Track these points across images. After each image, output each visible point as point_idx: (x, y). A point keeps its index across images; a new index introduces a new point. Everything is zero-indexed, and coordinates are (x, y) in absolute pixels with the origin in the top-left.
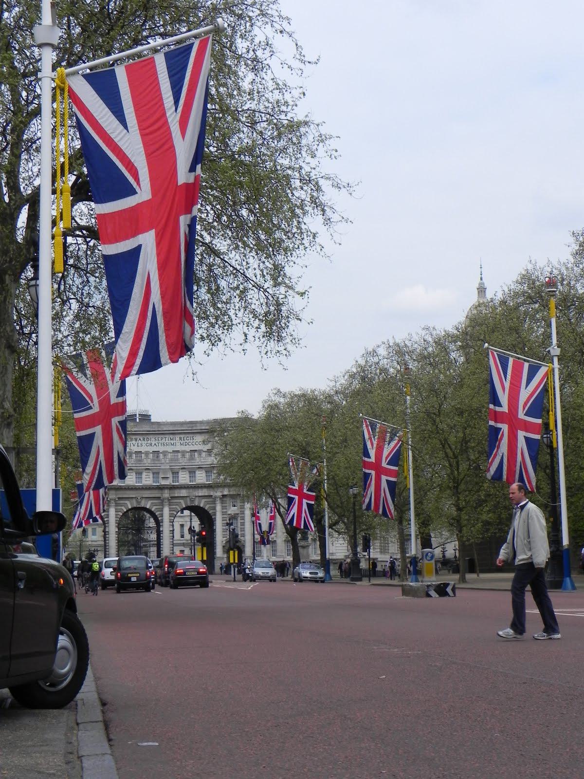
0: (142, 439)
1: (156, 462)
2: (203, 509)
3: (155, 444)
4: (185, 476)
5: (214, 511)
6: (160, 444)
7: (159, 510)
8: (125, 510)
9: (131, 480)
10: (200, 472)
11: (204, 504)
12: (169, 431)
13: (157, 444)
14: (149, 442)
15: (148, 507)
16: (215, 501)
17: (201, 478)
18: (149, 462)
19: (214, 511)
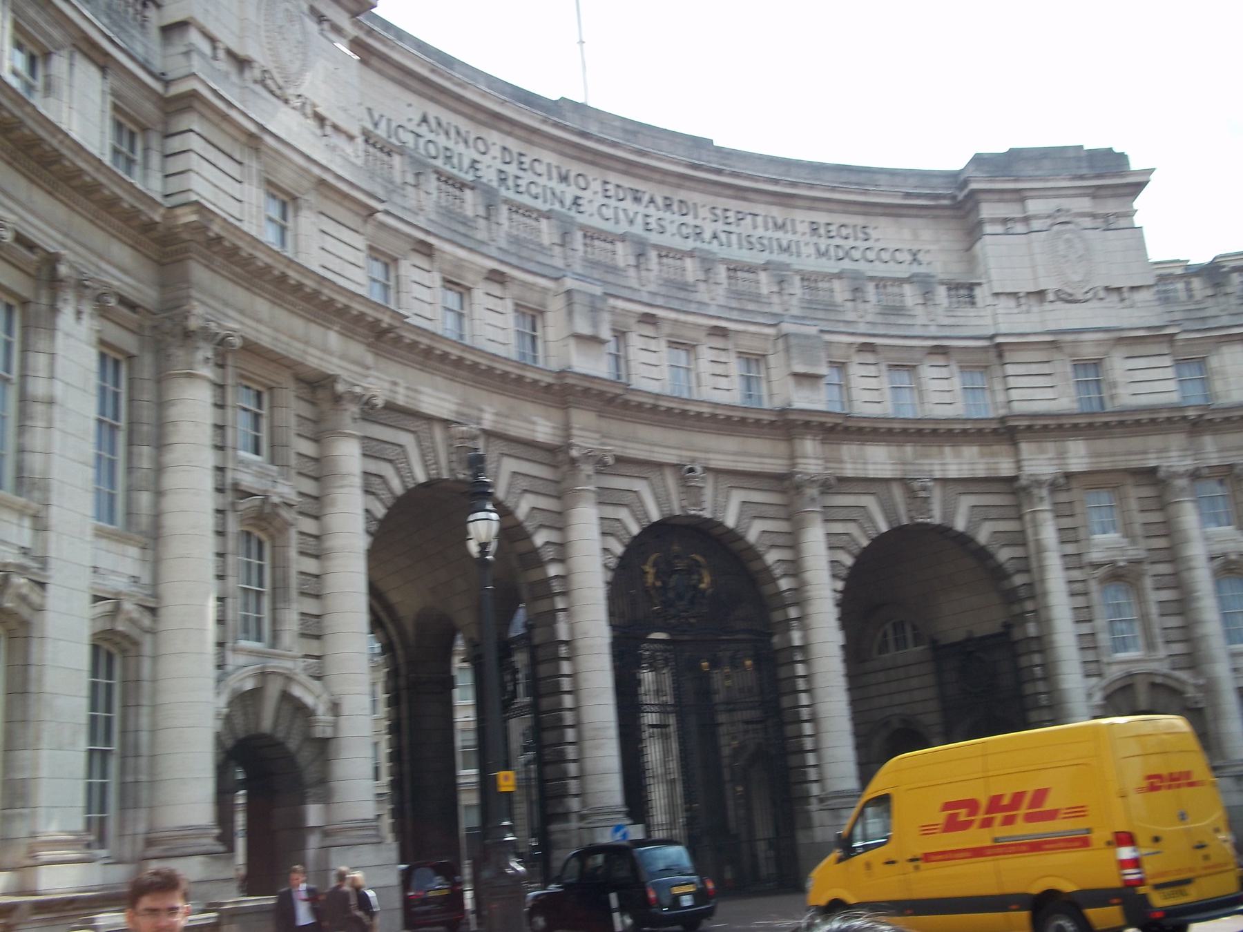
0: (660, 201)
1: (751, 306)
2: (964, 541)
3: (715, 237)
4: (873, 383)
5: (1018, 552)
6: (734, 238)
7: (780, 540)
8: (635, 530)
9: (654, 373)
10: (936, 372)
11: (970, 521)
12: (776, 182)
13: (723, 237)
14: (689, 219)
15: (730, 521)
16: (1018, 506)
17: (947, 398)
18: (722, 301)
19: (1018, 552)
